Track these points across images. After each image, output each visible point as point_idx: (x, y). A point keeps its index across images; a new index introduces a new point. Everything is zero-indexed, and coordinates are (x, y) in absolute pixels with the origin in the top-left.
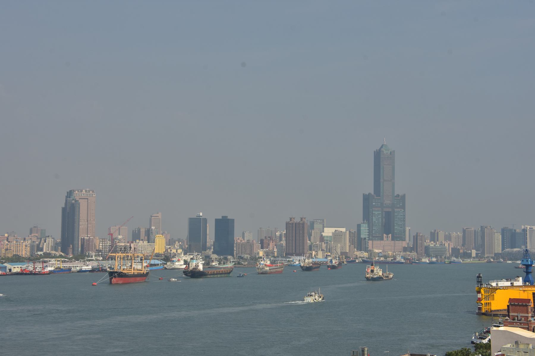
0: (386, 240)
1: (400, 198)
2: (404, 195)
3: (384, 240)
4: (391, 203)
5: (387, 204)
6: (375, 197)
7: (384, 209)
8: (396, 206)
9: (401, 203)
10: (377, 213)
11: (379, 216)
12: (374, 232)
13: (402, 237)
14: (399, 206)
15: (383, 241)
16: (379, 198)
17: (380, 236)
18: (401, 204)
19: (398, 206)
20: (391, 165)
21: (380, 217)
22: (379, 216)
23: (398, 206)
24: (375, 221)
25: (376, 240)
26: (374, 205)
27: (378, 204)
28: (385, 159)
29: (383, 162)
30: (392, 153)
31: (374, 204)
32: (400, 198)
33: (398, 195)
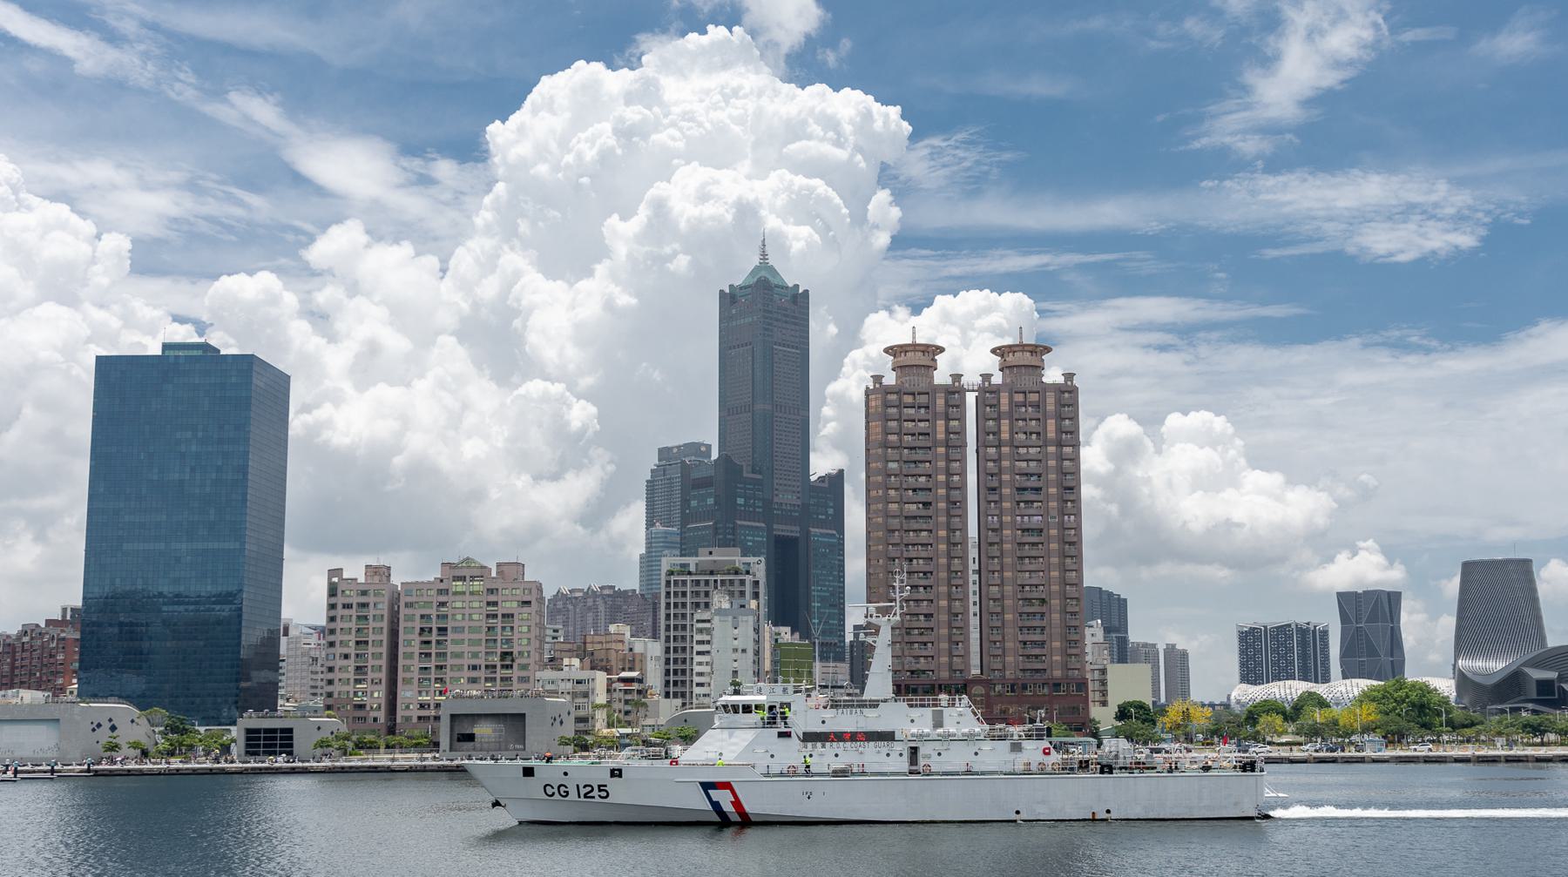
1: (826, 485)
2: (841, 472)
4: (799, 502)
5: (784, 507)
6: (745, 475)
7: (775, 526)
8: (815, 516)
9: (831, 507)
13: (835, 644)
14: (824, 517)
16: (759, 477)
18: (831, 511)
19: (820, 517)
20: (797, 348)
23: (820, 517)
28: (777, 320)
29: (772, 331)
30: (799, 301)
31: (740, 501)
32: (826, 485)
33: (822, 479)
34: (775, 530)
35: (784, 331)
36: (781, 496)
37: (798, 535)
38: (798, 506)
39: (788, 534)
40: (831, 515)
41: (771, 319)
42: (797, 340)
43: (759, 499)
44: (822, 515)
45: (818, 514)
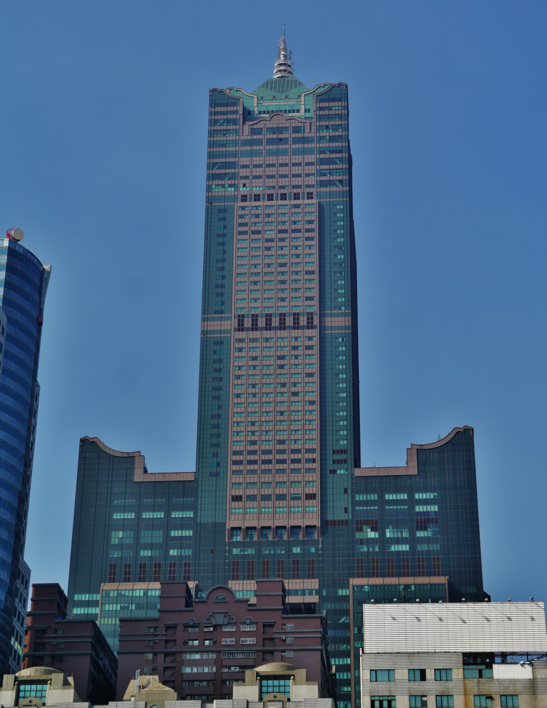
20: (310, 196)
41: (235, 154)
42: (311, 180)
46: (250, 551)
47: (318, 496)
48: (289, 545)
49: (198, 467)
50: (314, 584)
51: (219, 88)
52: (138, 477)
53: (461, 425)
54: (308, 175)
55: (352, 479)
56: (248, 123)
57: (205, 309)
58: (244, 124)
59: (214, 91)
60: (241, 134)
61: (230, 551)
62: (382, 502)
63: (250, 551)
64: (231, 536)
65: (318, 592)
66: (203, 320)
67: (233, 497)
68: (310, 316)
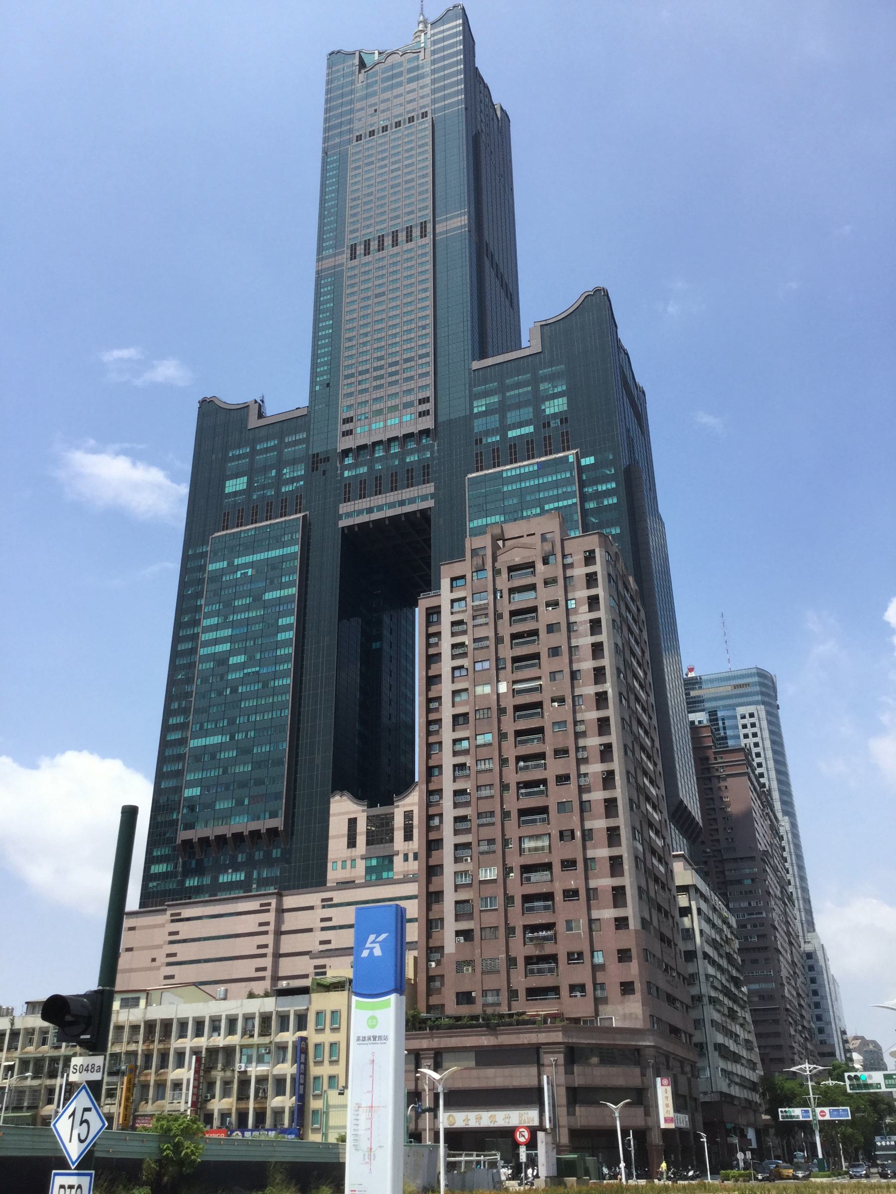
0: (359, 871)
3: (334, 875)
4: (428, 423)
7: (344, 508)
10: (251, 565)
11: (268, 596)
12: (196, 791)
14: (530, 429)
15: (313, 898)
17: (272, 832)
18: (556, 406)
19: (511, 434)
21: (280, 601)
22: (268, 596)
23: (511, 434)
24: (221, 660)
25: (231, 886)
26: (235, 494)
27: (280, 481)
34: (349, 515)
35: (383, 106)
36: (359, 430)
37: (430, 503)
38: (426, 432)
39: (398, 511)
40: (554, 416)
43: (293, 462)
44: (520, 425)
45: (503, 429)
46: (363, 470)
47: (432, 400)
48: (402, 456)
49: (311, 402)
50: (429, 488)
51: (336, 49)
52: (253, 422)
53: (590, 287)
54: (422, 97)
55: (470, 374)
56: (363, 71)
57: (320, 249)
58: (360, 72)
59: (333, 53)
60: (356, 82)
61: (342, 474)
62: (502, 390)
63: (363, 470)
64: (342, 461)
65: (433, 496)
66: (318, 260)
67: (344, 420)
68: (423, 226)
